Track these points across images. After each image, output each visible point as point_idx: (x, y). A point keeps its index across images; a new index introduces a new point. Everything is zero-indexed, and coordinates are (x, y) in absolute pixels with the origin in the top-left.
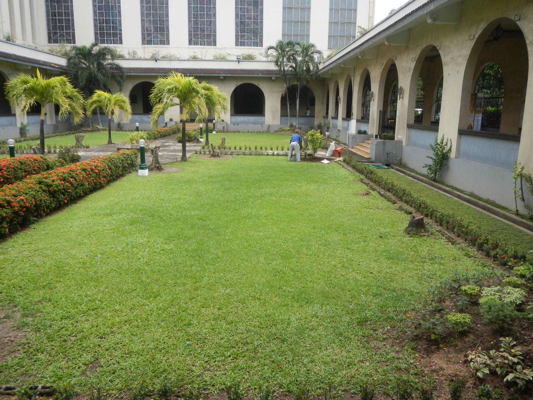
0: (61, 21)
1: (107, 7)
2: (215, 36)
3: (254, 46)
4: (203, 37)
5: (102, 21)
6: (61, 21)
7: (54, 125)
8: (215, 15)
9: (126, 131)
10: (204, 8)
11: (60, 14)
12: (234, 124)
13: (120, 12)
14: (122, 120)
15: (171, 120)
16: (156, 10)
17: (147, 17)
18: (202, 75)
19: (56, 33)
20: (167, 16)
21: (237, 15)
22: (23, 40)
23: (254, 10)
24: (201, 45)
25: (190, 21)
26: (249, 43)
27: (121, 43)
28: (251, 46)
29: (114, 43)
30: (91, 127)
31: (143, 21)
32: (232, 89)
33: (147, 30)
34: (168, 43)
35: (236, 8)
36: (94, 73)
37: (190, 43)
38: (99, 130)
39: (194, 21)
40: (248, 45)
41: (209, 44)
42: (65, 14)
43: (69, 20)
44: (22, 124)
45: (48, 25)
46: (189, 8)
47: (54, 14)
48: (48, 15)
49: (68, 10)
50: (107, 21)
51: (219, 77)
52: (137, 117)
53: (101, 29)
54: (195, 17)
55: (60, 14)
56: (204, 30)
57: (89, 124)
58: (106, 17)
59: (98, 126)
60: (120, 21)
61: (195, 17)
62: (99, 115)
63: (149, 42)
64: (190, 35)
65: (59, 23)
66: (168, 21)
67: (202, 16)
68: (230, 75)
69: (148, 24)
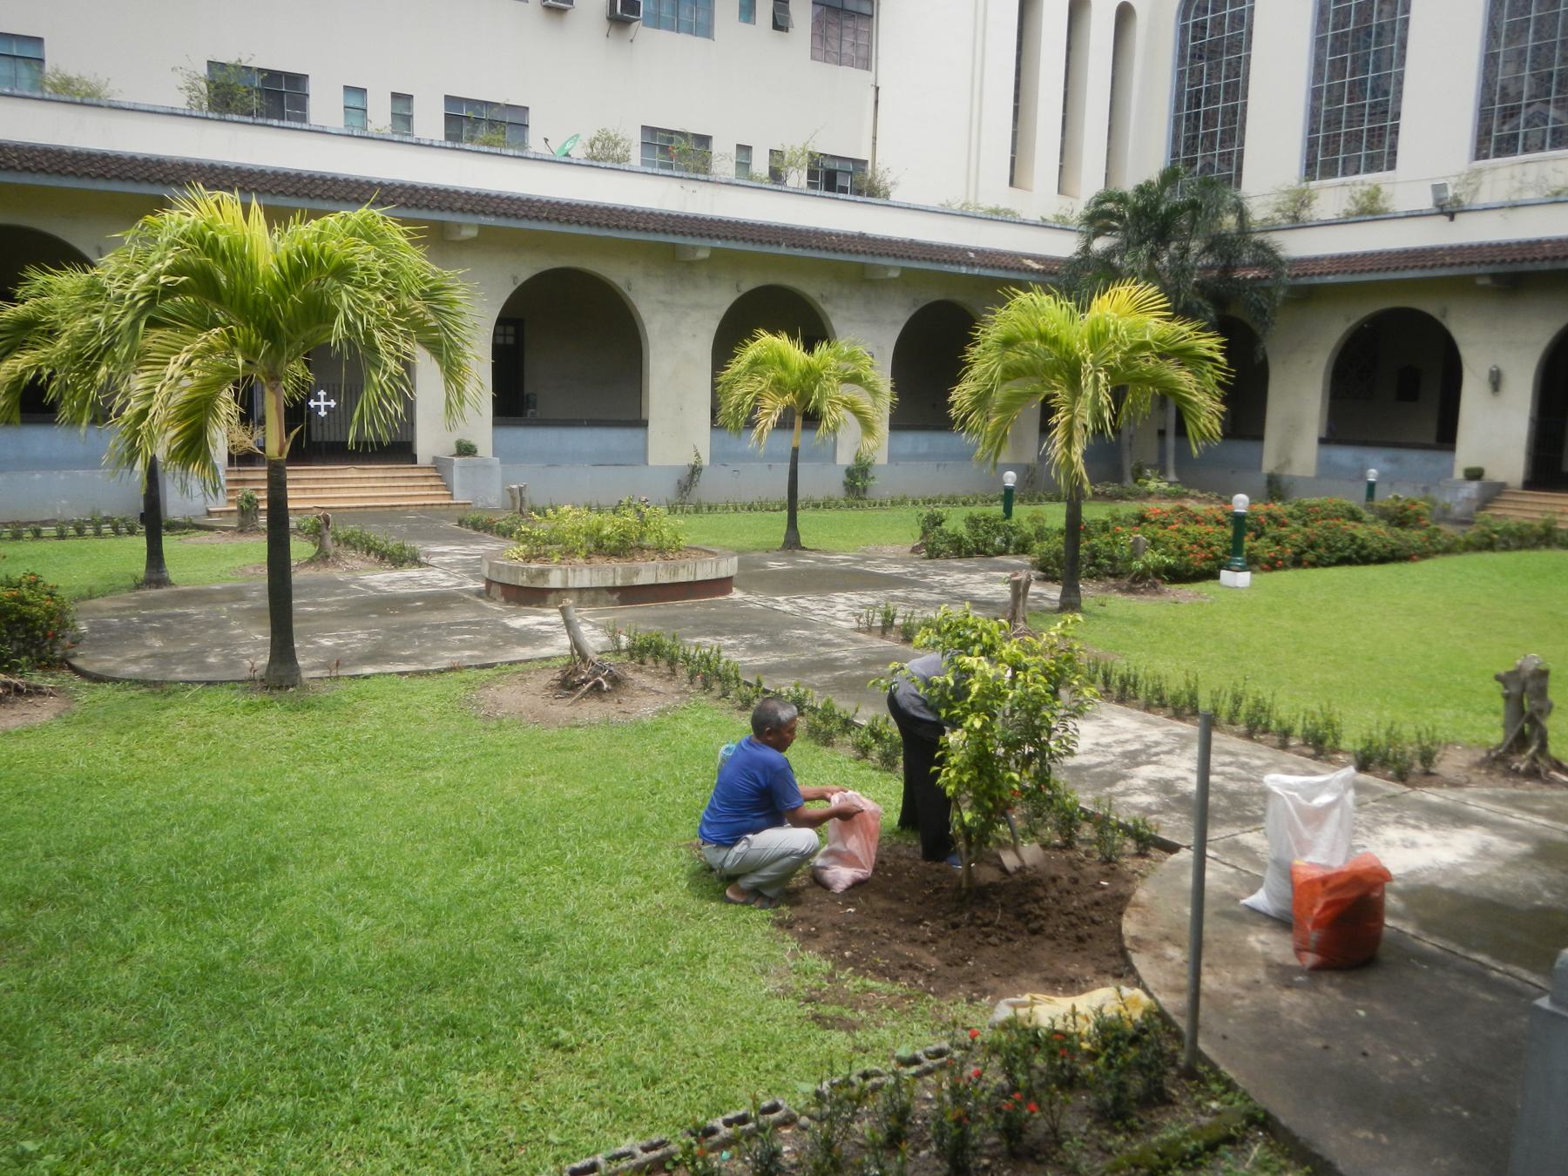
0: (1210, 118)
7: (1028, 467)
13: (1403, 46)
14: (1289, 462)
15: (1474, 474)
22: (1060, 191)
27: (1392, 166)
29: (1367, 171)
30: (1128, 482)
31: (1490, 60)
33: (1505, 96)
42: (1226, 92)
43: (1234, 109)
44: (858, 459)
47: (1195, 100)
48: (1178, 108)
49: (1237, 75)
52: (1345, 456)
53: (1333, 121)
55: (1212, 95)
60: (1400, 82)
63: (1507, 146)
65: (1206, 126)
69: (1511, 68)
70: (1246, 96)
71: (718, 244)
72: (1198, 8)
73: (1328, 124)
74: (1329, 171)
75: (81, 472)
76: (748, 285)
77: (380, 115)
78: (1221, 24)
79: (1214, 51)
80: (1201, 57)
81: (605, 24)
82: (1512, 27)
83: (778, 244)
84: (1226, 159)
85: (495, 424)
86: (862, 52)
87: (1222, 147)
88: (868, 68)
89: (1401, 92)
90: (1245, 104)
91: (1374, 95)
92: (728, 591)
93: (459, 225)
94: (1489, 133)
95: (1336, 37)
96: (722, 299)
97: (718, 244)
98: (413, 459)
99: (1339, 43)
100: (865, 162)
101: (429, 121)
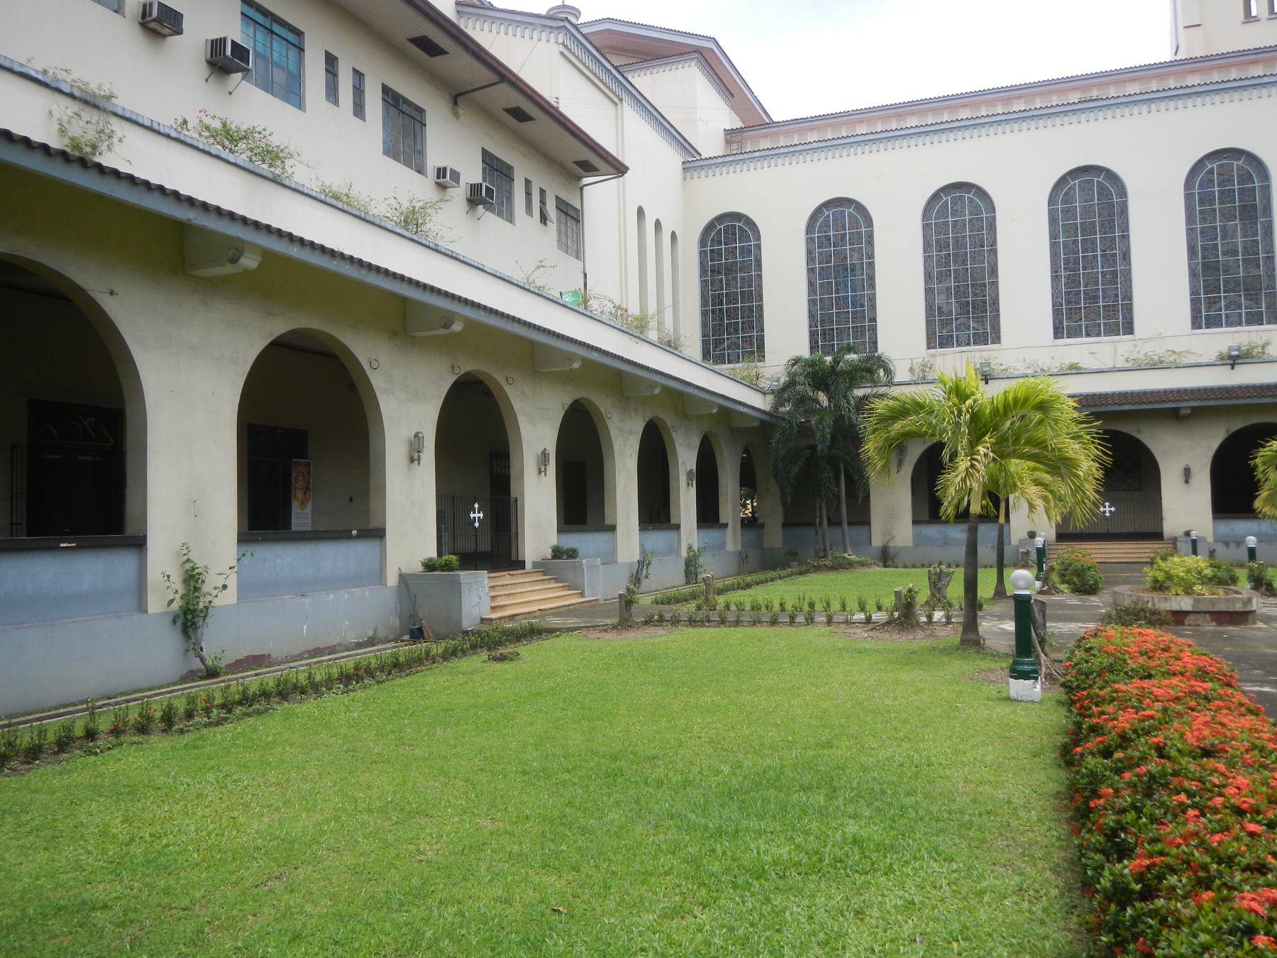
0: (732, 313)
1: (842, 268)
2: (1129, 309)
3: (1249, 323)
4: (1093, 313)
5: (827, 303)
6: (732, 313)
8: (1126, 256)
9: (905, 567)
10: (1093, 242)
11: (731, 298)
12: (1227, 544)
13: (872, 278)
14: (892, 538)
16: (964, 262)
17: (940, 282)
18: (1126, 407)
19: (722, 341)
20: (994, 271)
21: (1192, 250)
23: (1244, 231)
24: (1088, 335)
25: (1055, 278)
26: (1236, 319)
28: (1240, 324)
30: (830, 558)
31: (929, 292)
32: (1215, 443)
34: (997, 339)
35: (1190, 231)
36: (849, 418)
37: (1058, 333)
38: (850, 565)
39: (1068, 277)
40: (1229, 324)
41: (1112, 330)
42: (743, 297)
43: (751, 309)
44: (690, 548)
45: (704, 325)
46: (1054, 246)
47: (718, 300)
48: (704, 302)
49: (750, 286)
50: (841, 302)
51: (1177, 410)
53: (827, 319)
54: (1071, 265)
56: (1096, 298)
57: (825, 551)
58: (837, 292)
59: (846, 555)
60: (872, 299)
61: (1071, 265)
62: (845, 525)
63: (945, 342)
64: (1057, 312)
65: (729, 317)
66: (995, 284)
67: (1090, 262)
68: (1213, 403)
69: (943, 297)
70: (761, 300)
72: (713, 240)
75: (358, 591)
79: (730, 269)
82: (940, 273)
85: (560, 531)
91: (854, 306)
96: (638, 426)
98: (521, 565)
99: (824, 273)
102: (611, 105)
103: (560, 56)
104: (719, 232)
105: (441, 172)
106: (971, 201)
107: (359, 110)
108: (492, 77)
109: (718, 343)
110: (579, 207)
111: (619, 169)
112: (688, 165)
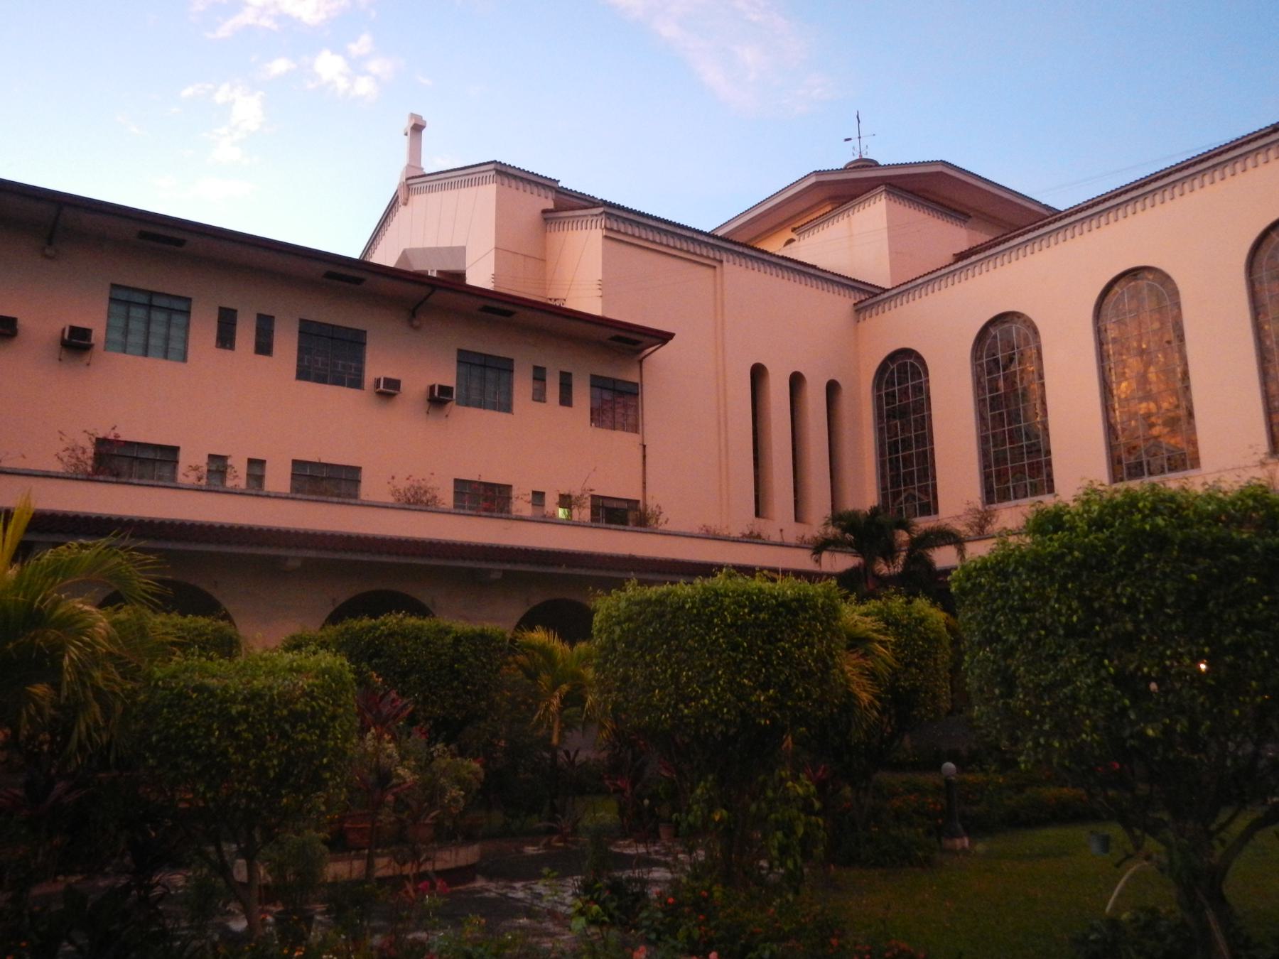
0: (908, 460)
22: (798, 519)
29: (1032, 495)
42: (917, 441)
43: (925, 453)
47: (894, 447)
49: (923, 428)
53: (1001, 460)
55: (906, 444)
58: (1009, 424)
71: (508, 567)
73: (997, 462)
74: (1004, 497)
76: (537, 600)
77: (238, 476)
78: (906, 393)
79: (903, 413)
80: (895, 417)
81: (427, 405)
83: (560, 565)
84: (924, 490)
86: (631, 420)
87: (919, 481)
88: (636, 431)
89: (1048, 435)
90: (933, 449)
91: (1028, 438)
92: (473, 880)
93: (286, 558)
94: (1120, 462)
95: (992, 399)
97: (508, 567)
99: (995, 403)
100: (638, 502)
101: (278, 478)
102: (709, 272)
103: (609, 243)
104: (892, 372)
105: (378, 381)
106: (1151, 288)
107: (264, 347)
108: (424, 291)
109: (898, 494)
110: (636, 380)
111: (664, 337)
112: (860, 306)
